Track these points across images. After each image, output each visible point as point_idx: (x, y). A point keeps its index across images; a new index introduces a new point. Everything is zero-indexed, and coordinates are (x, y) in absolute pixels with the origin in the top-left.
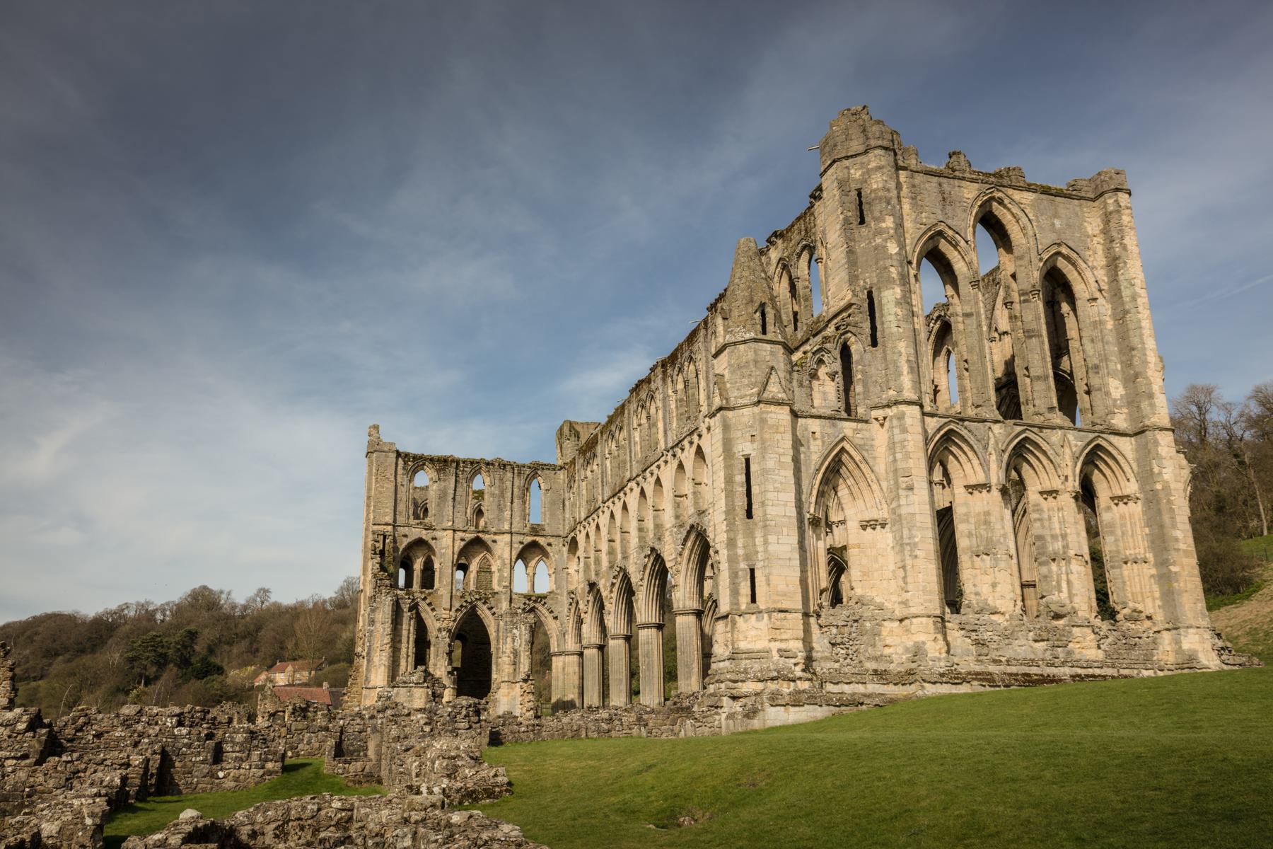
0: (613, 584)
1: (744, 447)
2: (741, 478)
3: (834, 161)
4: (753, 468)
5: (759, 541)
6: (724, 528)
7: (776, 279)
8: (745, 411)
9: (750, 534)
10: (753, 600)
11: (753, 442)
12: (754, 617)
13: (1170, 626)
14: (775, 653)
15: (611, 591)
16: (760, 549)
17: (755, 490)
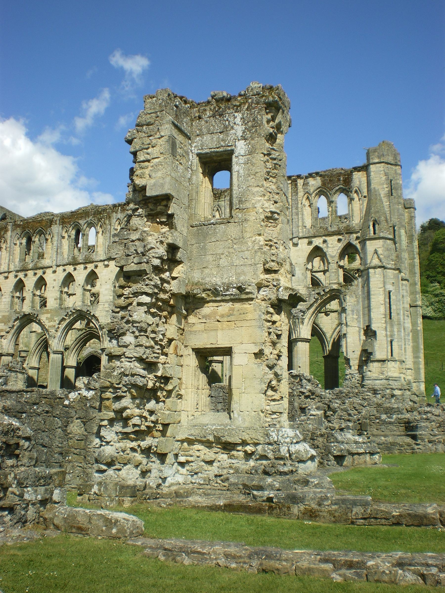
0: (63, 319)
1: (390, 287)
2: (388, 300)
3: (383, 162)
4: (393, 297)
5: (396, 330)
6: (383, 322)
7: (313, 195)
8: (390, 271)
9: (392, 326)
10: (392, 355)
11: (393, 286)
12: (393, 363)
13: (416, 381)
14: (402, 379)
15: (59, 324)
16: (396, 333)
17: (393, 307)
